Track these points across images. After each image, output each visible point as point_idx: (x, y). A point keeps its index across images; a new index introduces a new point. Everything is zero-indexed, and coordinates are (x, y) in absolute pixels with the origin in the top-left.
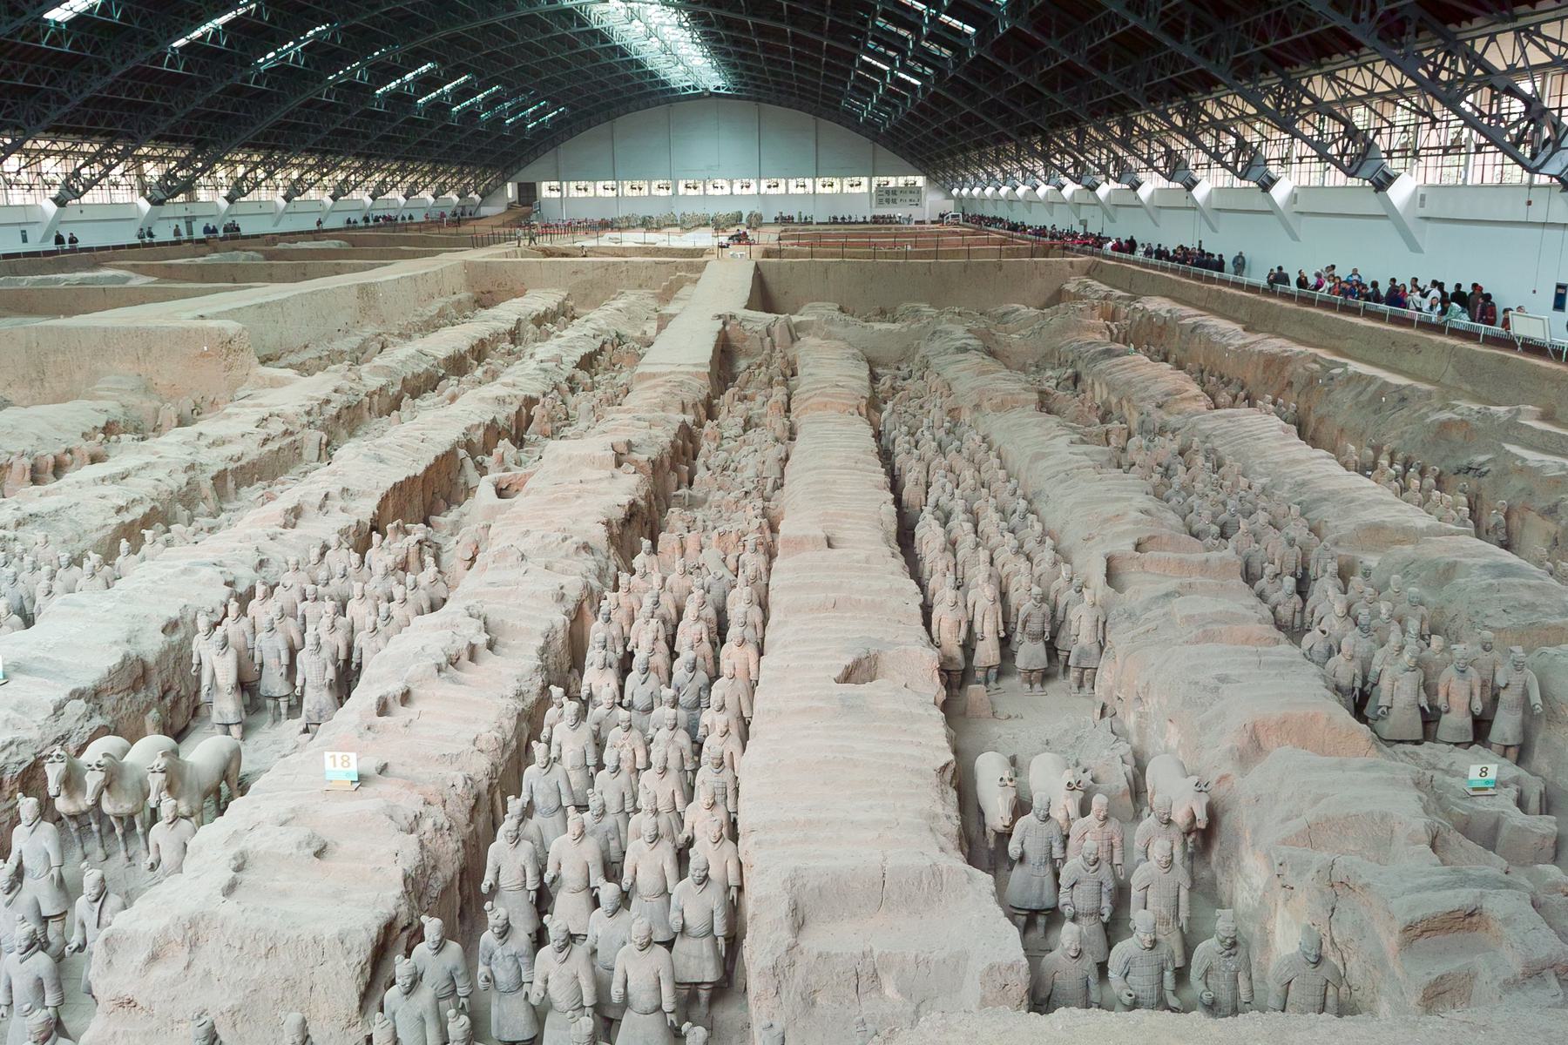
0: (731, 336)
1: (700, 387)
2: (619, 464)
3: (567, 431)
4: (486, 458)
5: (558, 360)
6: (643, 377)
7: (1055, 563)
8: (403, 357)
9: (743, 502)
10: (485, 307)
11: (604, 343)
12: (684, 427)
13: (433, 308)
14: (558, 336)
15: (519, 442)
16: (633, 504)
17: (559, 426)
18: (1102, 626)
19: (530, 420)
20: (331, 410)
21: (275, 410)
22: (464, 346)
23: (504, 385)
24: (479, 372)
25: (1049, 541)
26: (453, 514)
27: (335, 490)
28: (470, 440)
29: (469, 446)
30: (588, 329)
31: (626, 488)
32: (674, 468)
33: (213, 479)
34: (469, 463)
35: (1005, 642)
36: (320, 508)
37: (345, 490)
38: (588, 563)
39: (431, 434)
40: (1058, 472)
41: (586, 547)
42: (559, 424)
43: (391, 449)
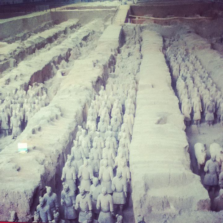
1: (117, 45)
3: (80, 58)
4: (58, 65)
5: (77, 38)
7: (216, 91)
8: (35, 38)
10: (57, 24)
11: (90, 33)
14: (77, 32)
15: (67, 60)
16: (99, 77)
17: (78, 56)
19: (70, 55)
20: (17, 53)
22: (51, 35)
23: (63, 45)
24: (56, 42)
29: (54, 62)
32: (109, 67)
34: (54, 67)
35: (202, 114)
36: (15, 79)
37: (21, 74)
38: (87, 93)
41: (87, 89)
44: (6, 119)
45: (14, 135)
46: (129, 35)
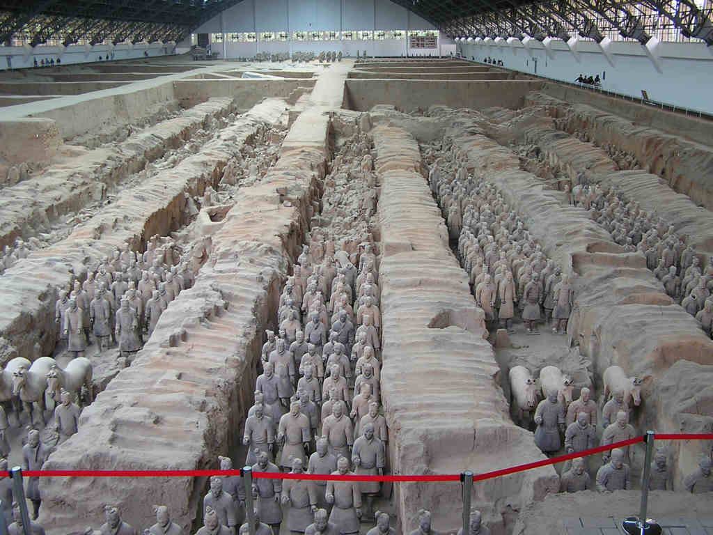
0: (335, 125)
1: (319, 157)
2: (282, 202)
4: (200, 198)
5: (234, 139)
6: (286, 149)
9: (354, 224)
10: (186, 108)
11: (258, 129)
12: (314, 178)
13: (156, 108)
14: (232, 125)
15: (216, 187)
16: (292, 225)
18: (572, 294)
20: (107, 170)
21: (77, 170)
24: (187, 147)
25: (538, 246)
26: (184, 232)
27: (121, 217)
28: (190, 187)
29: (190, 190)
30: (248, 121)
31: (286, 217)
33: (46, 211)
34: (191, 200)
38: (272, 260)
39: (168, 184)
40: (540, 206)
41: (271, 250)
42: (238, 177)
43: (147, 192)
44: (104, 314)
45: (122, 348)
46: (344, 135)
